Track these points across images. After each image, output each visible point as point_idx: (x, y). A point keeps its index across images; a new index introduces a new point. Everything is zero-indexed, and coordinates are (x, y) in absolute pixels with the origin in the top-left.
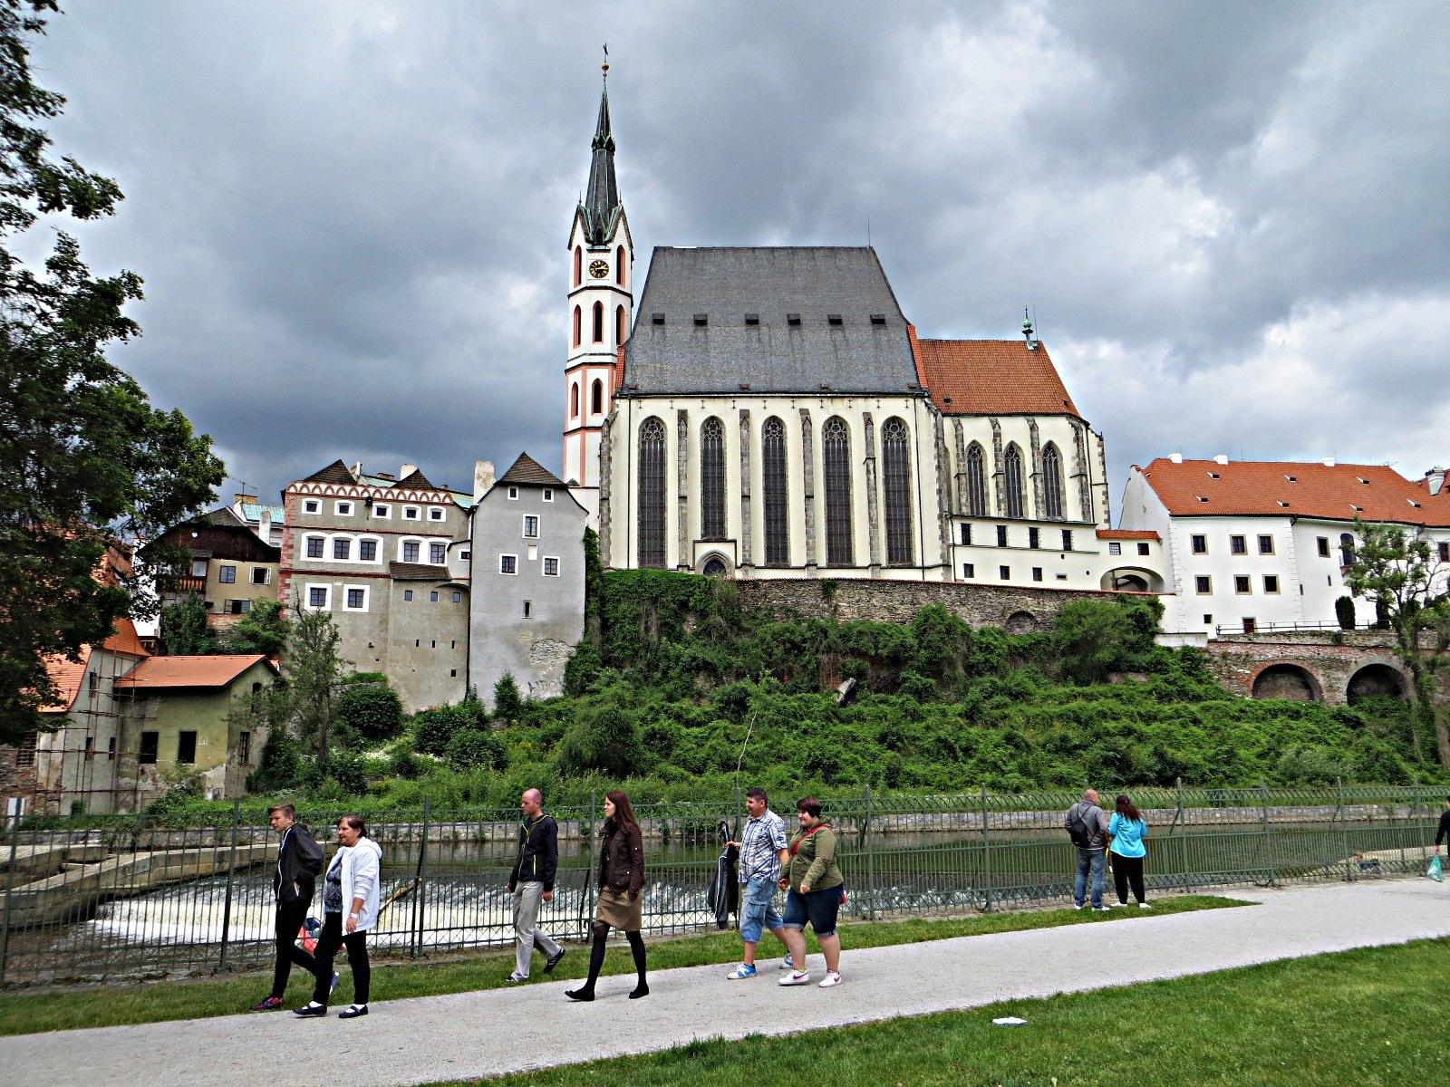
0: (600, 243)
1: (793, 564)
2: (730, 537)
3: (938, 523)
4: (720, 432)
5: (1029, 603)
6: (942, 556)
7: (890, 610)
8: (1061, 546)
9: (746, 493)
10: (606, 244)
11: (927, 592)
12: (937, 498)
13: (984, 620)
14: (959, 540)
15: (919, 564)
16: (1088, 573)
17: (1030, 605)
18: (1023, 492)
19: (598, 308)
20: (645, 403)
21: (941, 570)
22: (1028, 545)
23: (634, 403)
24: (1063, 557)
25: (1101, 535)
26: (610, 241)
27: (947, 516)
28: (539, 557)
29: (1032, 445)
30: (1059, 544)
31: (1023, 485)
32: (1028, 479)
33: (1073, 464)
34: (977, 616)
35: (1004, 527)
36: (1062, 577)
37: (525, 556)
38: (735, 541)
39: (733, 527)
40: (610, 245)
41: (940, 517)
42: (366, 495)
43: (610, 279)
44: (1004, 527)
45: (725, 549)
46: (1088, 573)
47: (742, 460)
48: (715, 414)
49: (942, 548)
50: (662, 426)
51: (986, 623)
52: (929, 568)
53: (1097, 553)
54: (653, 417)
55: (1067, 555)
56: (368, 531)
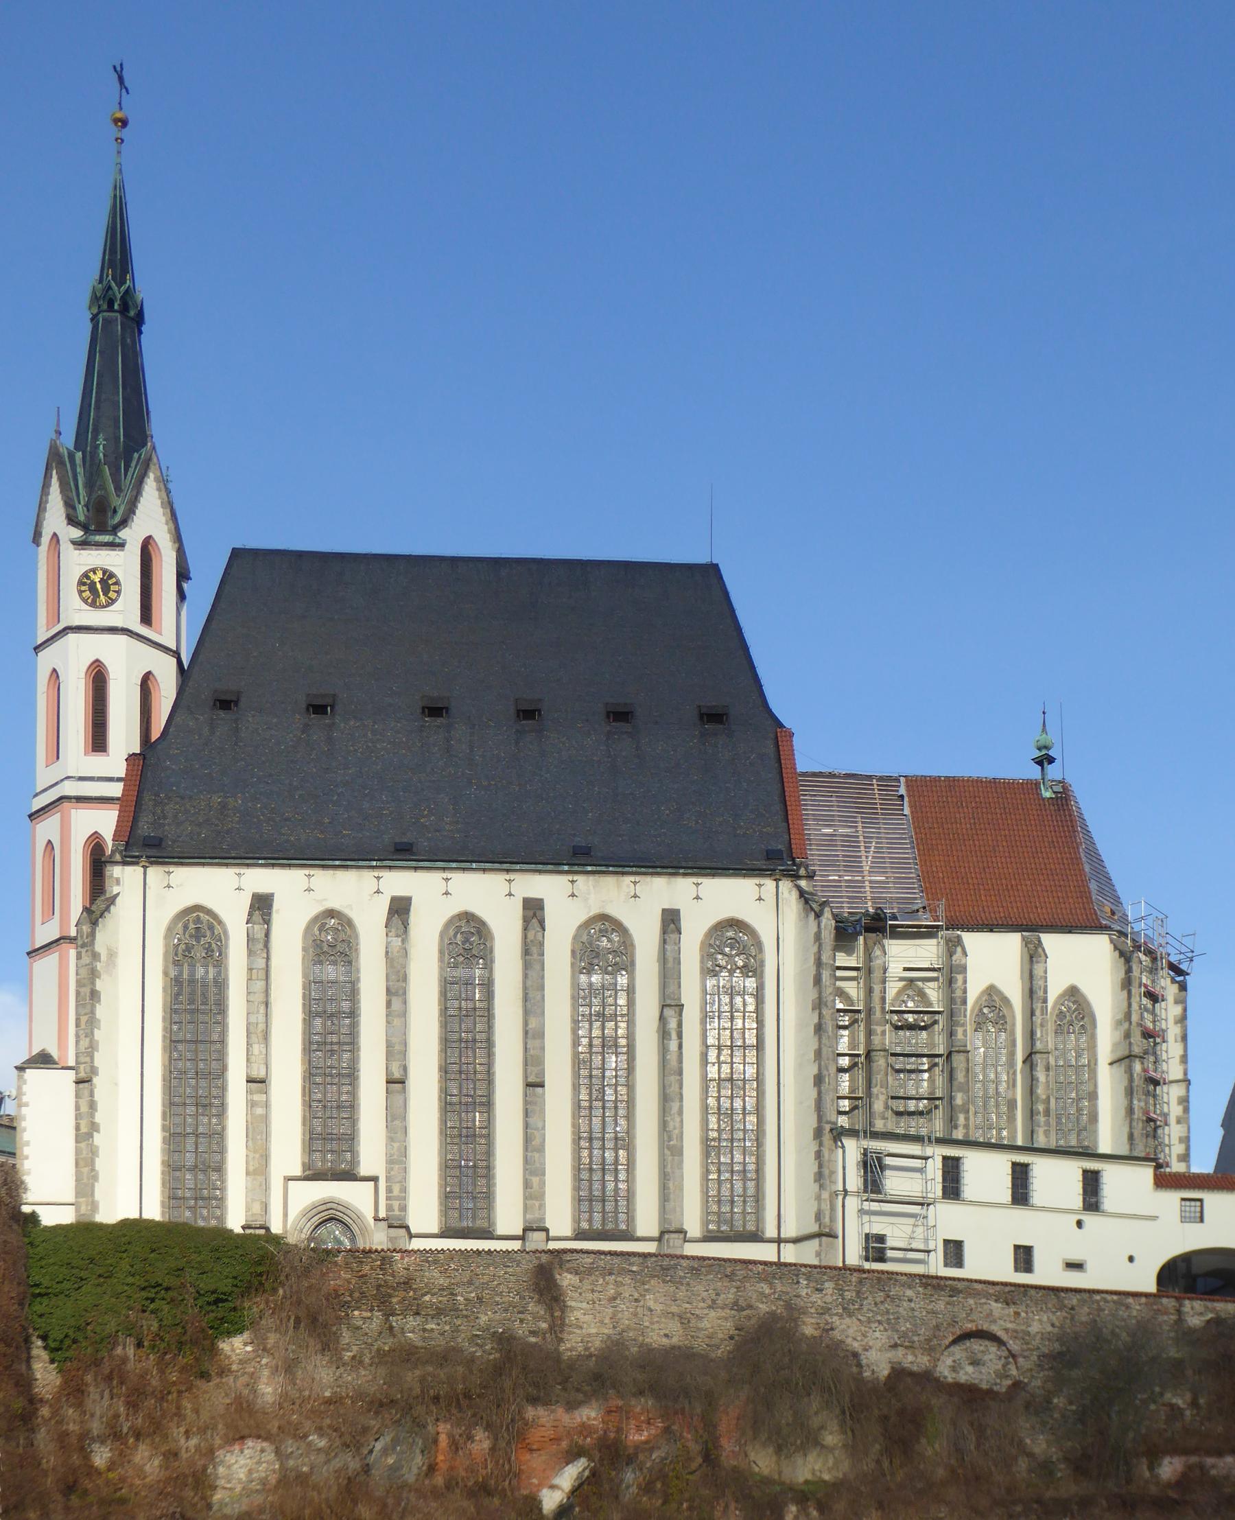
0: (101, 530)
1: (500, 1231)
2: (363, 1171)
5: (996, 1314)
8: (1078, 1202)
9: (397, 1075)
10: (115, 530)
11: (771, 1285)
13: (895, 1346)
16: (1131, 1259)
17: (999, 1318)
20: (182, 874)
22: (1007, 1197)
24: (1079, 1224)
25: (1165, 1181)
26: (124, 523)
27: (829, 1134)
30: (1074, 1195)
34: (879, 1337)
35: (957, 1160)
36: (519, 705)
38: (375, 1179)
39: (371, 1153)
40: (123, 534)
43: (126, 610)
44: (957, 1160)
46: (1131, 1259)
47: (389, 1004)
51: (900, 1352)
52: (787, 1241)
55: (1089, 1219)
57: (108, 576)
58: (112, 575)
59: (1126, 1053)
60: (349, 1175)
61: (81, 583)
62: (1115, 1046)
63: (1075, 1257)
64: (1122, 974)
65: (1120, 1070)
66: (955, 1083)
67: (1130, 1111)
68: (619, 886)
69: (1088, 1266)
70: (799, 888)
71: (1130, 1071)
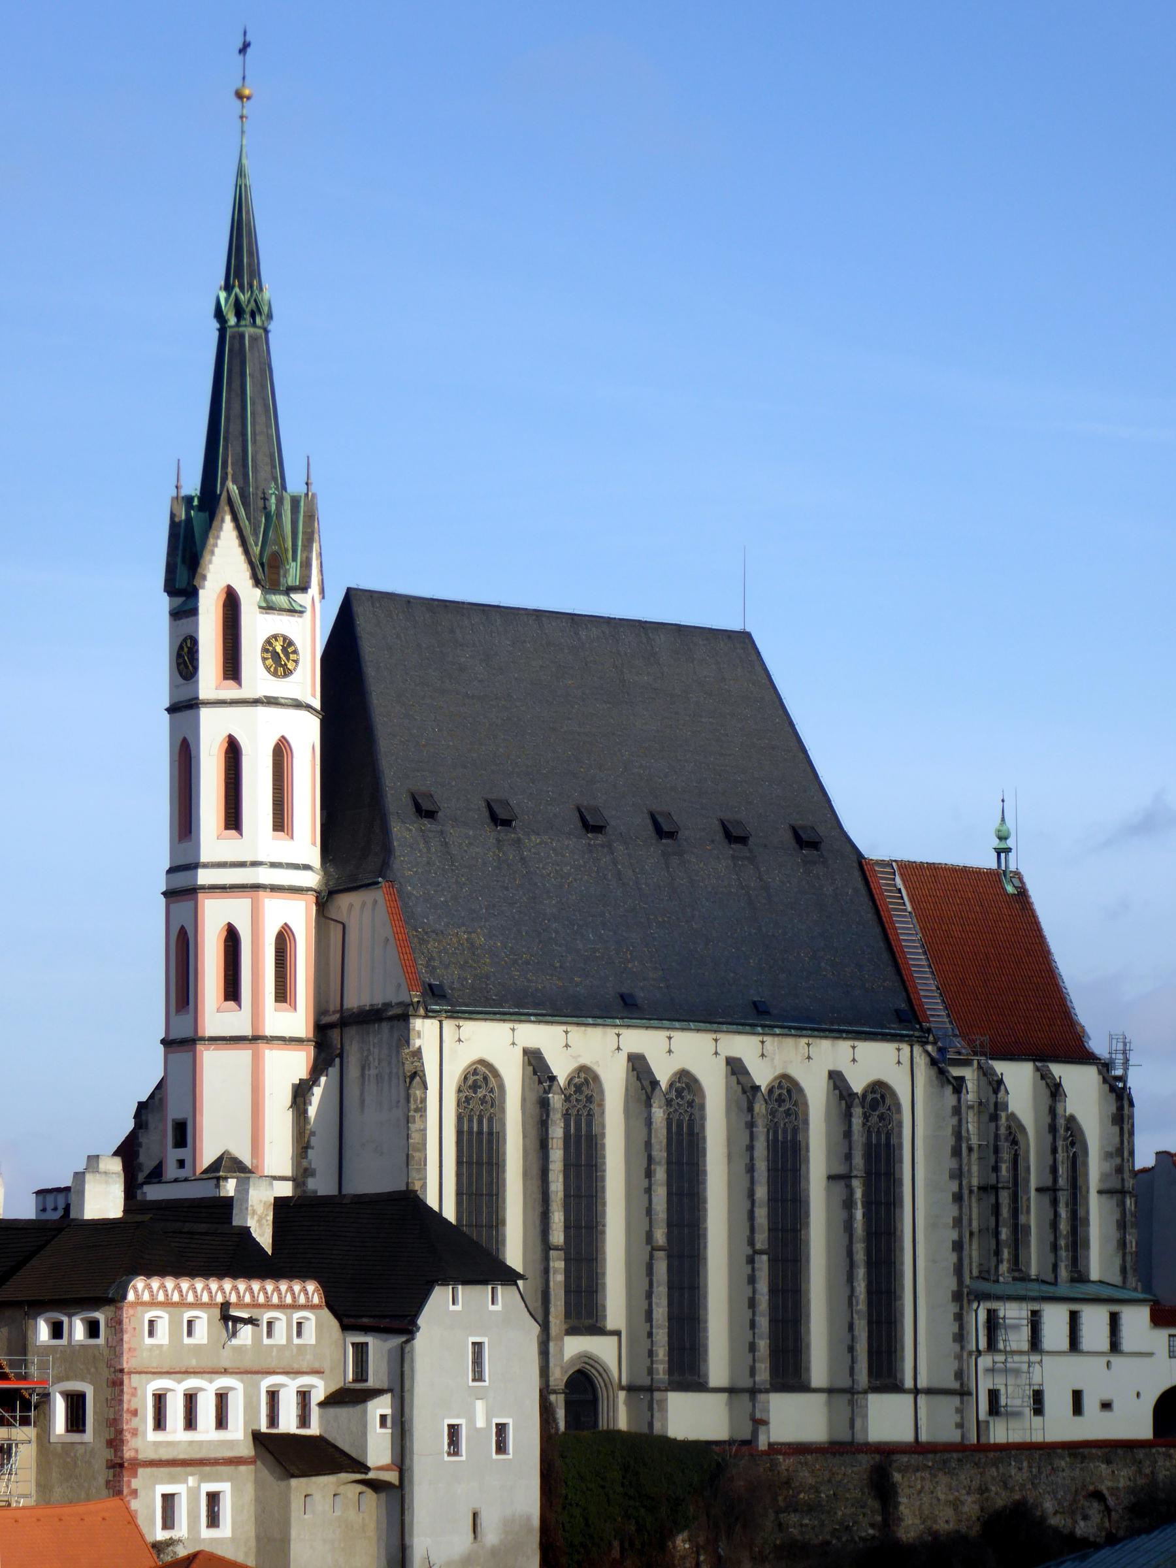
2: (611, 1325)
3: (953, 1308)
4: (590, 1099)
6: (959, 1375)
7: (956, 1504)
12: (954, 1258)
14: (983, 1344)
15: (909, 1383)
18: (1022, 1219)
19: (281, 753)
21: (955, 1401)
23: (449, 1025)
28: (488, 1421)
29: (1053, 1129)
31: (1022, 1203)
32: (1033, 1193)
33: (1108, 1167)
37: (472, 1420)
38: (617, 1333)
41: (957, 1297)
42: (220, 1299)
45: (603, 1349)
48: (586, 1060)
49: (959, 1357)
50: (493, 1082)
53: (1150, 1354)
54: (482, 1062)
55: (1116, 1360)
56: (225, 1372)
57: (288, 643)
58: (291, 643)
59: (1119, 1186)
60: (597, 1329)
61: (264, 650)
62: (1104, 1177)
63: (1106, 1397)
64: (1113, 1109)
65: (1111, 1203)
66: (1001, 1219)
67: (1122, 1244)
68: (796, 1048)
69: (1115, 1406)
70: (927, 1052)
71: (1122, 1204)
